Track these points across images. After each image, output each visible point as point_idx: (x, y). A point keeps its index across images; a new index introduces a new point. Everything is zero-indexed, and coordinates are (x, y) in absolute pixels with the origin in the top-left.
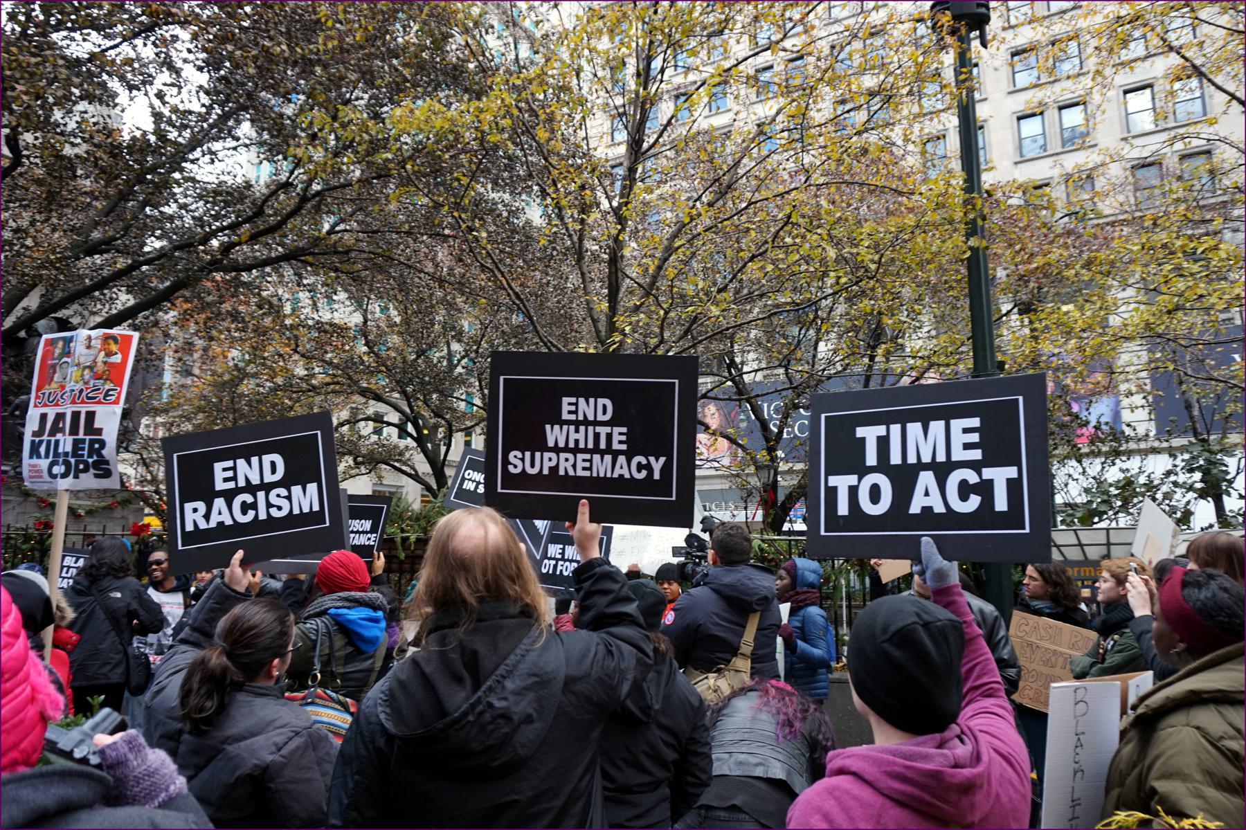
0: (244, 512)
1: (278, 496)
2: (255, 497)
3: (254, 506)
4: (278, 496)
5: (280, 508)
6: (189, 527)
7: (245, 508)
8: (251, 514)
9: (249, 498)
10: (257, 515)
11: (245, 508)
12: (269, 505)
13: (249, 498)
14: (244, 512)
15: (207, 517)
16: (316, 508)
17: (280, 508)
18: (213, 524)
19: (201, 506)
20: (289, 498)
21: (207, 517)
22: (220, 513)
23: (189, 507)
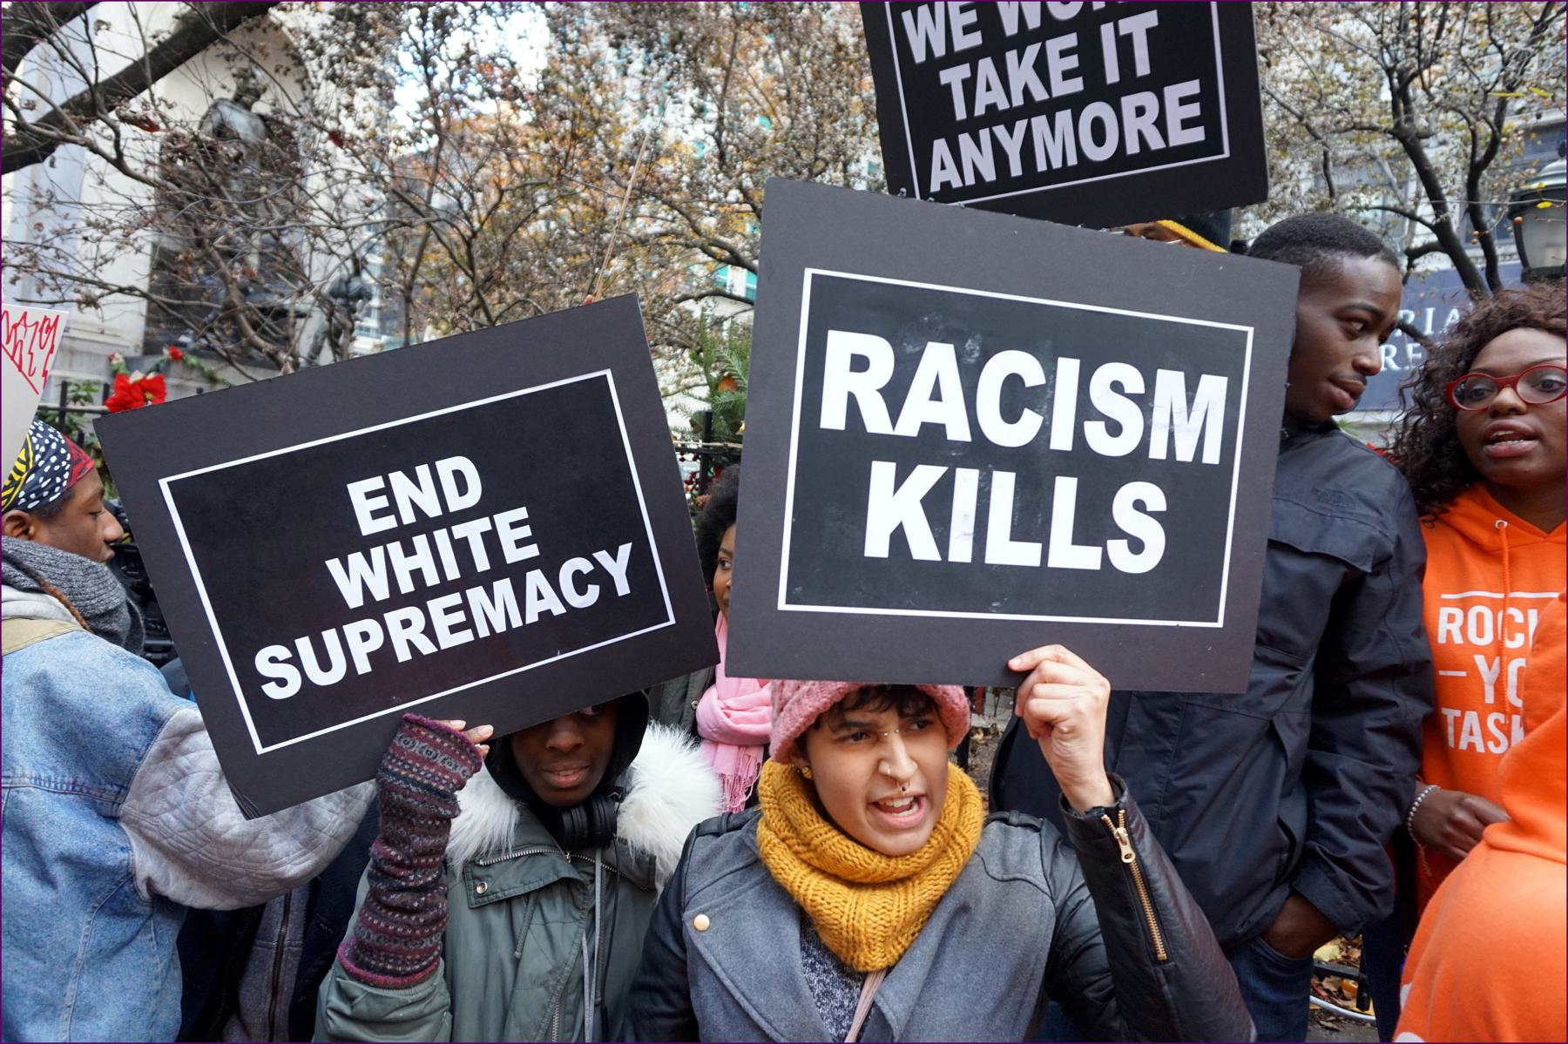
0: (1010, 414)
1: (1117, 387)
2: (1051, 372)
3: (1041, 399)
4: (1117, 387)
5: (1114, 429)
6: (833, 417)
7: (1015, 398)
8: (1030, 422)
9: (1030, 370)
10: (1046, 430)
11: (1015, 398)
12: (1086, 409)
13: (1030, 370)
14: (1010, 414)
15: (894, 396)
16: (1212, 456)
17: (1114, 429)
18: (908, 426)
19: (880, 351)
20: (1144, 402)
21: (894, 396)
22: (936, 395)
23: (842, 345)
